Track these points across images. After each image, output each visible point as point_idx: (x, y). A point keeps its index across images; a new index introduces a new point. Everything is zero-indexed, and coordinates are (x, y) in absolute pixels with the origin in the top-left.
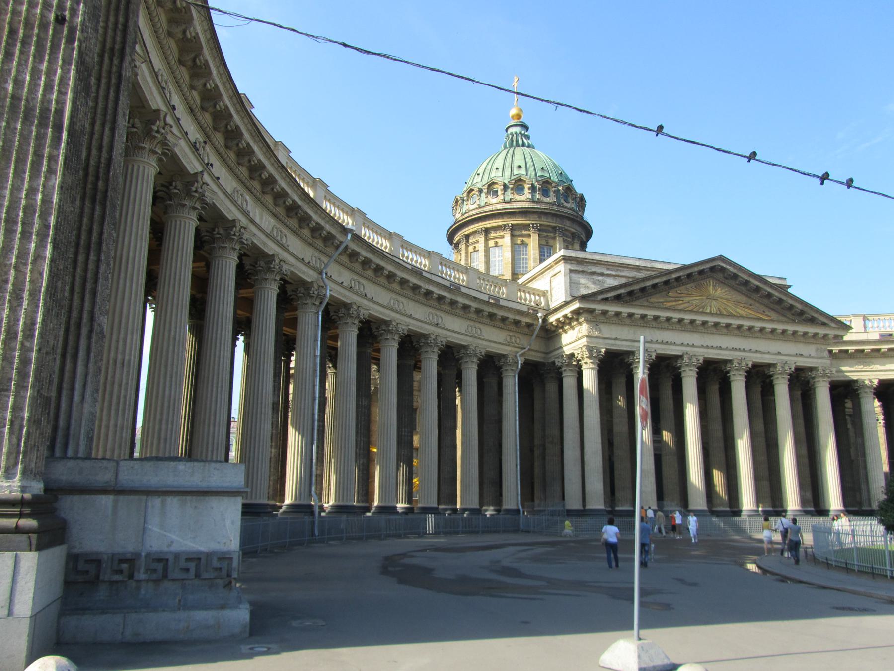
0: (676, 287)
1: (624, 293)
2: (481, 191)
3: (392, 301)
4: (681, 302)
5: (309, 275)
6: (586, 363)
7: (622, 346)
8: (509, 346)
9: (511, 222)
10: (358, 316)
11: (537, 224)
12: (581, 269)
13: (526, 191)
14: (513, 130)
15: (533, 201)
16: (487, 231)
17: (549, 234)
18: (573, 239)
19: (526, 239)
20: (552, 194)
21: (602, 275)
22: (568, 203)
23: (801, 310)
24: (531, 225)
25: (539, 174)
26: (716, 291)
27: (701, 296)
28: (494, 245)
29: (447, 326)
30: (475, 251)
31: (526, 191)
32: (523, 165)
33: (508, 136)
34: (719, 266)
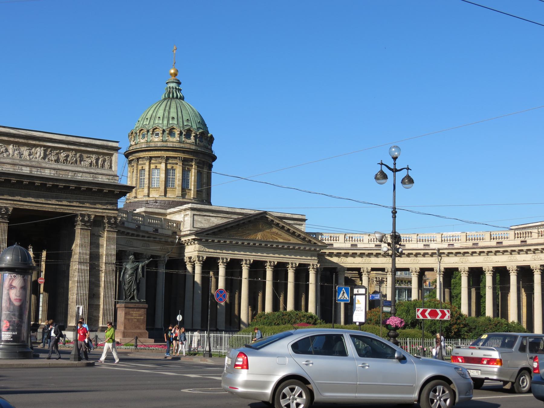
1: (217, 231)
2: (148, 131)
4: (245, 233)
6: (197, 263)
8: (162, 251)
9: (166, 155)
11: (182, 157)
12: (199, 214)
13: (177, 136)
14: (172, 85)
16: (151, 158)
20: (192, 137)
21: (210, 216)
22: (202, 142)
24: (178, 158)
25: (185, 123)
26: (263, 227)
28: (155, 168)
30: (143, 169)
31: (177, 136)
32: (175, 117)
33: (167, 89)
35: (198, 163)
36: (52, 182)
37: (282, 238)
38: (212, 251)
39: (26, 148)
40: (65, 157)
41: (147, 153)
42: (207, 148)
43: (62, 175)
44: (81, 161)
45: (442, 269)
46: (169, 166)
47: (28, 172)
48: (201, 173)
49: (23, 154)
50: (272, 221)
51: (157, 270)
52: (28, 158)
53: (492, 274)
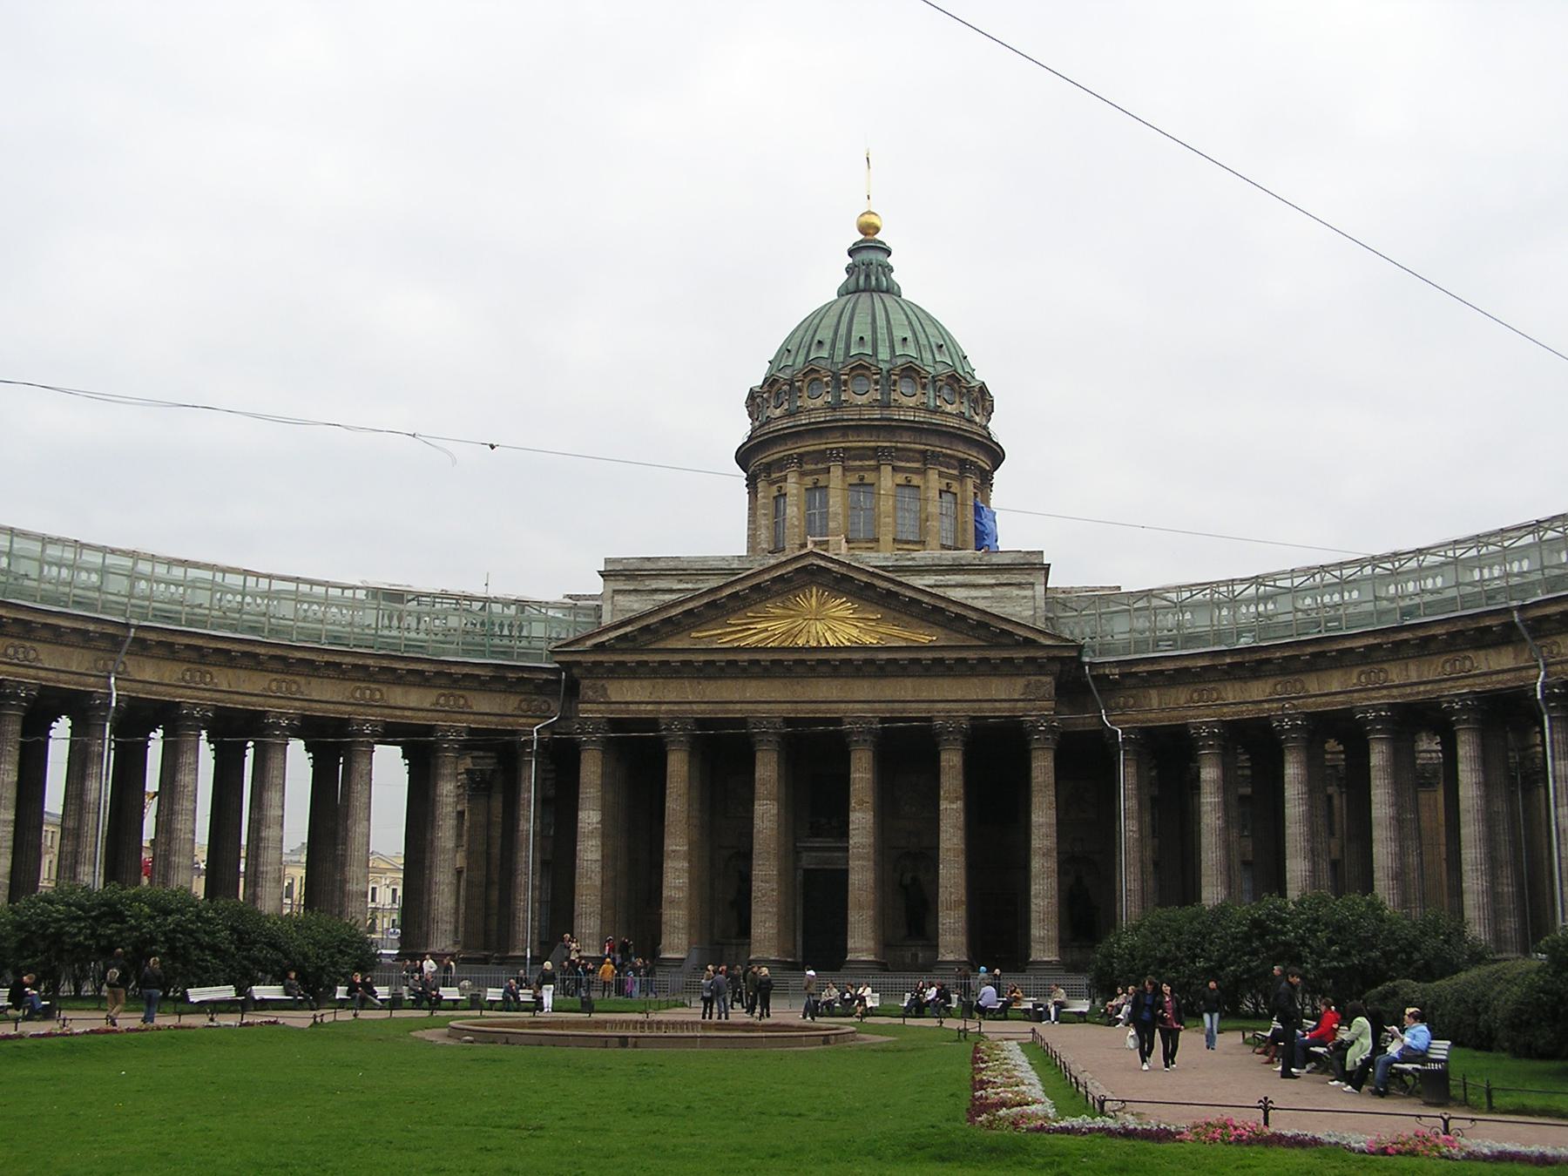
0: (745, 607)
1: (631, 632)
3: (274, 684)
5: (90, 685)
7: (640, 712)
9: (797, 451)
10: (190, 716)
12: (632, 588)
16: (768, 468)
17: (867, 463)
18: (925, 465)
19: (822, 478)
21: (671, 591)
23: (978, 621)
27: (791, 617)
29: (392, 703)
34: (812, 564)
42: (936, 410)
48: (919, 487)
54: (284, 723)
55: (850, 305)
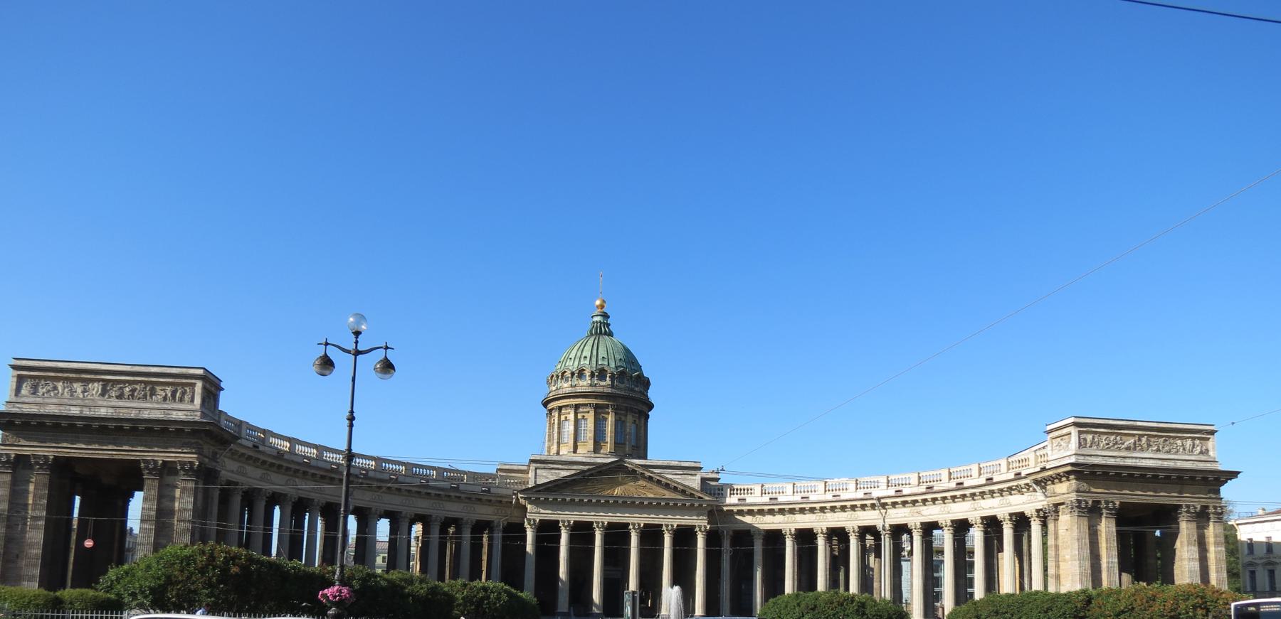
2: (557, 377)
15: (591, 385)
16: (560, 408)
22: (623, 383)
25: (600, 363)
31: (588, 378)
35: (616, 409)
36: (99, 422)
37: (652, 492)
38: (550, 512)
39: (80, 384)
40: (130, 391)
41: (557, 402)
42: (632, 390)
43: (123, 414)
44: (151, 396)
45: (887, 527)
46: (580, 416)
47: (78, 412)
49: (76, 392)
50: (634, 471)
51: (226, 526)
52: (81, 396)
53: (952, 531)
54: (408, 516)
55: (596, 341)
